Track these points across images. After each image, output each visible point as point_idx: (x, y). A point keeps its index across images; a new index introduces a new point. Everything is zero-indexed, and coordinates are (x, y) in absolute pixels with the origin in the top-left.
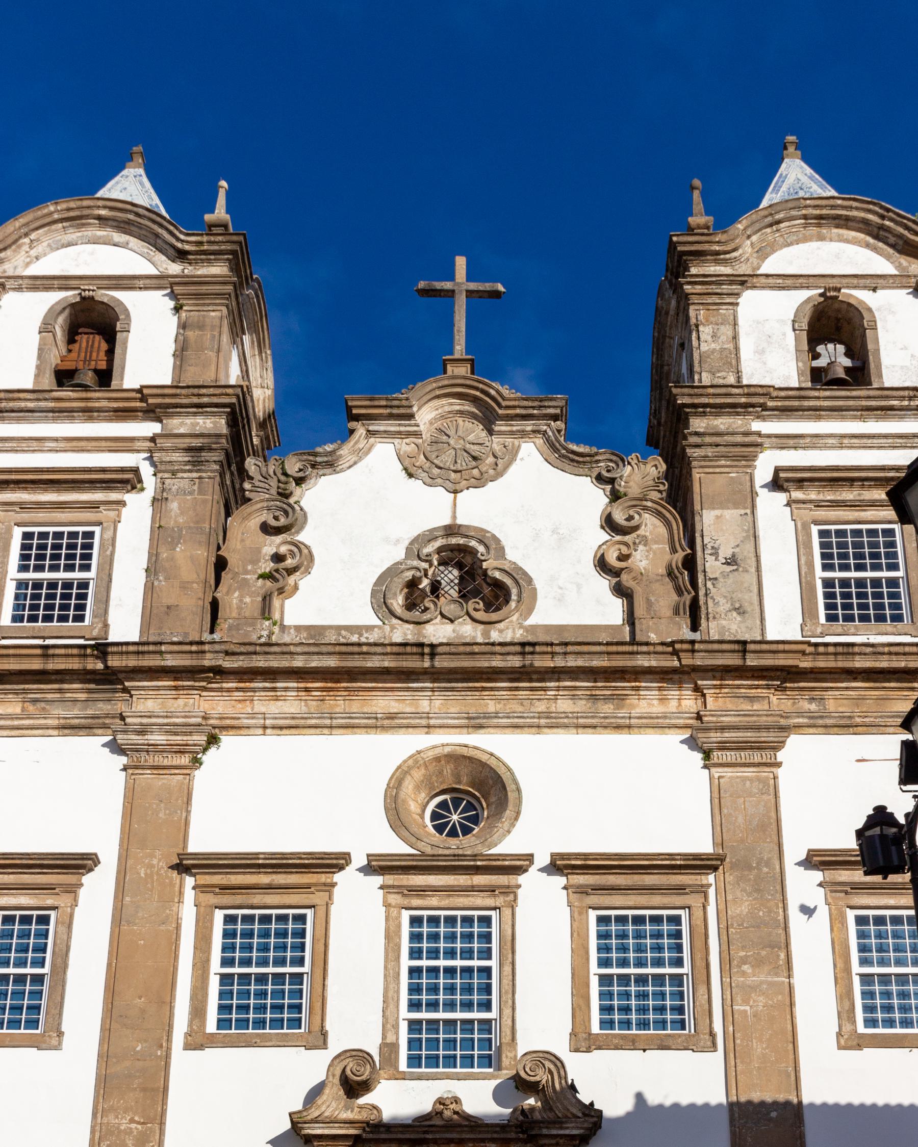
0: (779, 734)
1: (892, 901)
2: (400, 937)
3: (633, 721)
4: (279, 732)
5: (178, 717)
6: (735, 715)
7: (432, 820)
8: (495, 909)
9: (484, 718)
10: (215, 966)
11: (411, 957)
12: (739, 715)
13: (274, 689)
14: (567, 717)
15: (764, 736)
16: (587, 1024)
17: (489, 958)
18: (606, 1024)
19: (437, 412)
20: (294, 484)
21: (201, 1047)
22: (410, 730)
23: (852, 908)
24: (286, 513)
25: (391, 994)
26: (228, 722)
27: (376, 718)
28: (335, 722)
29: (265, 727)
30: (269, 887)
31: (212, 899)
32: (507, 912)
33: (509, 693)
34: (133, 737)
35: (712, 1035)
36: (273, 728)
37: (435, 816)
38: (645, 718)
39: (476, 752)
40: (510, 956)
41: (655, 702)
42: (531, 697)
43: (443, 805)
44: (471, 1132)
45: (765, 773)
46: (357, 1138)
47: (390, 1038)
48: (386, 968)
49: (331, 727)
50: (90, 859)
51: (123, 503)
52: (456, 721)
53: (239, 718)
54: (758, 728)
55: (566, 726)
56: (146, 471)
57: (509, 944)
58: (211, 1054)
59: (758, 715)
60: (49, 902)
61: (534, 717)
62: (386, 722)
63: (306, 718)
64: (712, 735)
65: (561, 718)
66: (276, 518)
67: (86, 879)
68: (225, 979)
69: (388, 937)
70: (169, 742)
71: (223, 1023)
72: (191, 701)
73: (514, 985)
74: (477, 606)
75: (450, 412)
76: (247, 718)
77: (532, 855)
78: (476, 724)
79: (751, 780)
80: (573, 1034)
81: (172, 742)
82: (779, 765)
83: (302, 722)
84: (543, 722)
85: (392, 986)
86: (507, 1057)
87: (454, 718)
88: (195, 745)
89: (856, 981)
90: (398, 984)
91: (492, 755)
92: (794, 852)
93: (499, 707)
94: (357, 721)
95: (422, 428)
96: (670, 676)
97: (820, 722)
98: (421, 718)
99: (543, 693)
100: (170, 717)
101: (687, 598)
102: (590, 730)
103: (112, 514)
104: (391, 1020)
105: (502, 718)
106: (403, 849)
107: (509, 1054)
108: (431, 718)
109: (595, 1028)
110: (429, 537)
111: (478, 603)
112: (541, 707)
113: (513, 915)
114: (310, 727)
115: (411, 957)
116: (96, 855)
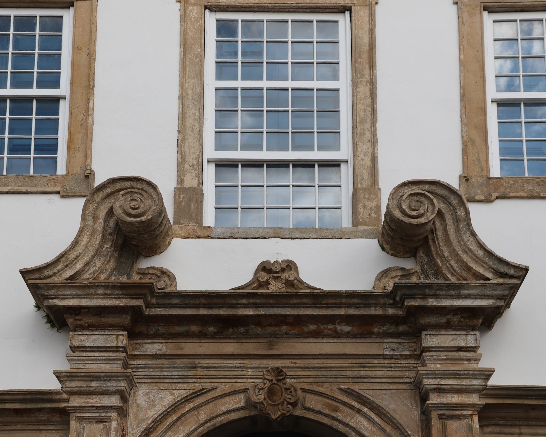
2: (203, 47)
16: (484, 164)
17: (336, 77)
25: (189, 122)
32: (361, 13)
40: (367, 72)
44: (314, 306)
47: (190, 182)
48: (182, 86)
57: (365, 57)
69: (185, 45)
73: (374, 111)
85: (191, 111)
86: (365, 207)
90: (201, 109)
104: (191, 159)
107: (367, 203)
113: (372, 16)
115: (219, 76)
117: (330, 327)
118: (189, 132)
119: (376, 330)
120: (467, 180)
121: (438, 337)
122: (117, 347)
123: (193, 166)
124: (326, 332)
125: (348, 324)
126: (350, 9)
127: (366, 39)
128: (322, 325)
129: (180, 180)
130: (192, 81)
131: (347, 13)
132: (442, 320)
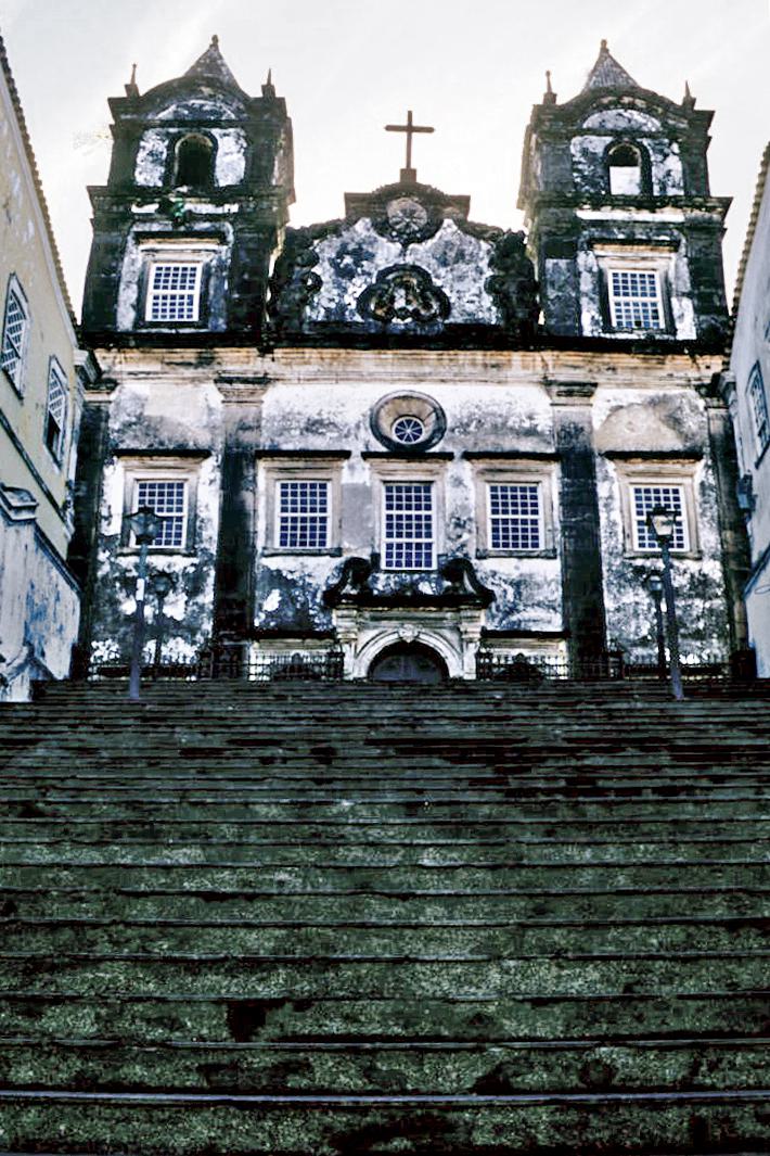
18: (495, 545)
23: (632, 484)
31: (276, 476)
37: (397, 430)
43: (401, 424)
78: (420, 378)
109: (489, 546)
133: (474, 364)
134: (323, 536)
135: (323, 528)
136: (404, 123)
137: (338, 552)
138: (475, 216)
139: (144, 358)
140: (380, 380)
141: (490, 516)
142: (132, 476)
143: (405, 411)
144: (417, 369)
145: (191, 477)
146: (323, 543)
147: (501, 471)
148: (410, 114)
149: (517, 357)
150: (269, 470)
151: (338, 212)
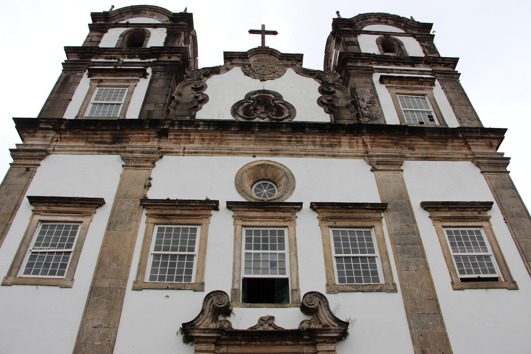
0: (401, 159)
1: (460, 224)
3: (340, 154)
4: (190, 155)
5: (148, 148)
6: (381, 152)
7: (255, 192)
8: (285, 227)
9: (277, 151)
10: (152, 250)
11: (246, 249)
12: (383, 152)
13: (189, 139)
14: (312, 151)
15: (395, 159)
18: (341, 280)
19: (256, 59)
20: (203, 76)
21: (140, 289)
22: (246, 155)
23: (444, 227)
24: (199, 84)
25: (237, 264)
26: (168, 150)
27: (232, 150)
28: (214, 151)
29: (184, 153)
30: (180, 215)
31: (154, 220)
32: (291, 228)
33: (287, 143)
34: (128, 154)
35: (394, 285)
36: (188, 153)
37: (256, 191)
38: (345, 152)
39: (274, 163)
40: (294, 248)
41: (348, 148)
42: (297, 144)
43: (259, 186)
45: (397, 174)
46: (218, 338)
49: (212, 153)
50: (100, 201)
51: (139, 81)
52: (266, 152)
53: (173, 149)
54: (392, 156)
55: (312, 155)
56: (149, 70)
57: (293, 242)
58: (145, 293)
59: (390, 152)
60: (79, 219)
61: (299, 151)
62: (236, 151)
63: (202, 149)
64: (374, 158)
65: (310, 152)
66: (196, 86)
67: (99, 211)
68: (156, 256)
70: (142, 156)
71: (152, 278)
72: (154, 143)
74: (273, 114)
75: (261, 59)
76: (177, 149)
77: (302, 203)
78: (275, 153)
79: (392, 176)
80: (328, 285)
81: (144, 157)
82: (402, 171)
83: (200, 151)
84: (302, 153)
87: (265, 151)
88: (154, 158)
89: (453, 258)
91: (281, 165)
92: (415, 204)
93: (283, 148)
94: (223, 151)
95: (251, 62)
96: (353, 137)
97: (415, 156)
98: (251, 150)
99: (301, 143)
100: (145, 148)
101: (355, 114)
102: (322, 157)
103: (134, 84)
105: (285, 151)
106: (243, 200)
108: (255, 150)
110: (254, 93)
111: (273, 113)
112: (302, 147)
113: (295, 229)
114: (203, 153)
115: (246, 249)
116: (103, 199)
117: (285, 342)
118: (236, 268)
119: (301, 343)
120: (328, 286)
121: (322, 347)
122: (211, 351)
123: (237, 280)
124: (283, 344)
125: (291, 341)
126: (288, 227)
127: (293, 237)
128: (282, 341)
129: (233, 286)
130: (237, 251)
131: (287, 228)
132: (323, 340)
133: (314, 143)
134: (189, 272)
135: (190, 265)
136: (260, 28)
137: (199, 287)
138: (306, 65)
139: (74, 138)
140: (245, 153)
141: (334, 254)
142: (38, 218)
143: (263, 176)
144: (273, 147)
145: (85, 220)
146: (189, 278)
147: (341, 218)
148: (263, 26)
149: (345, 140)
150: (146, 214)
151: (220, 61)
